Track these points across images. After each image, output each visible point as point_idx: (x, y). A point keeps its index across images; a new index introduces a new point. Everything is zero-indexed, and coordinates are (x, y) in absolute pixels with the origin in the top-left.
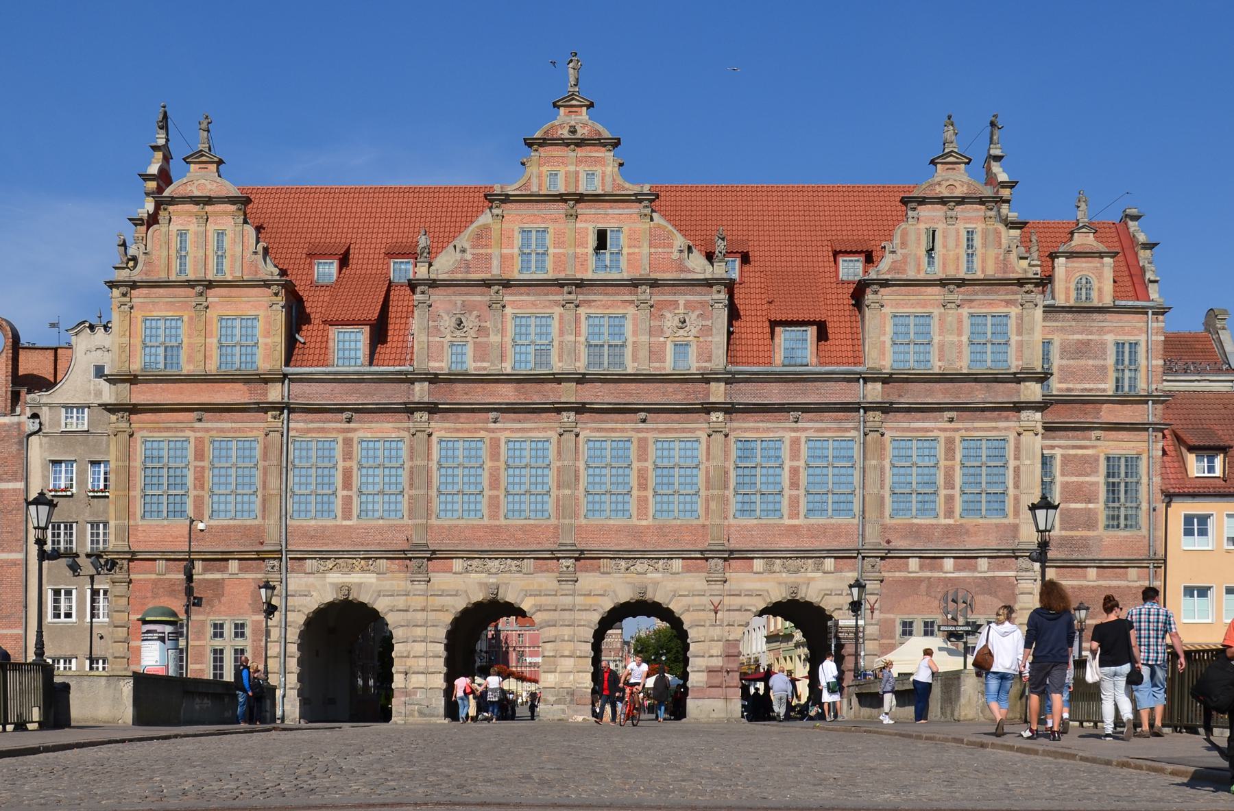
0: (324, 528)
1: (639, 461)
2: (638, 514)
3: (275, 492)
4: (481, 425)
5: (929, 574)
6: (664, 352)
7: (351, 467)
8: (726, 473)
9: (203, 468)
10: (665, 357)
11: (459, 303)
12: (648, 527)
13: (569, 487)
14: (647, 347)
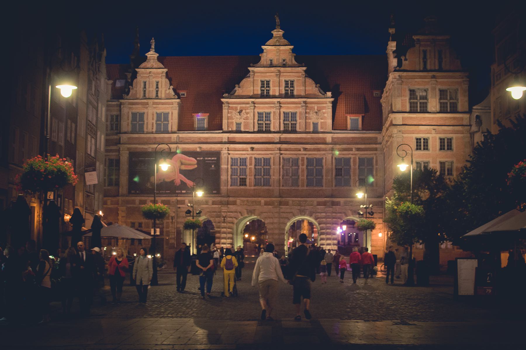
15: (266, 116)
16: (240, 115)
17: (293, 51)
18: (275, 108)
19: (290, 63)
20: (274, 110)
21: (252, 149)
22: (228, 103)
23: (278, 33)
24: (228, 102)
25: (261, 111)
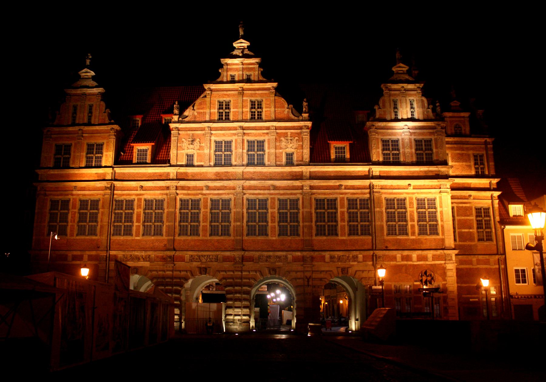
0: (127, 240)
1: (271, 208)
2: (271, 234)
3: (106, 224)
4: (199, 192)
5: (405, 263)
6: (282, 157)
7: (140, 212)
8: (311, 214)
9: (75, 212)
10: (282, 159)
11: (191, 135)
12: (276, 240)
13: (239, 221)
14: (275, 154)
15: (225, 145)
16: (193, 144)
17: (260, 65)
18: (236, 136)
19: (256, 79)
20: (236, 137)
21: (208, 188)
22: (178, 129)
23: (241, 44)
24: (178, 128)
25: (219, 139)
